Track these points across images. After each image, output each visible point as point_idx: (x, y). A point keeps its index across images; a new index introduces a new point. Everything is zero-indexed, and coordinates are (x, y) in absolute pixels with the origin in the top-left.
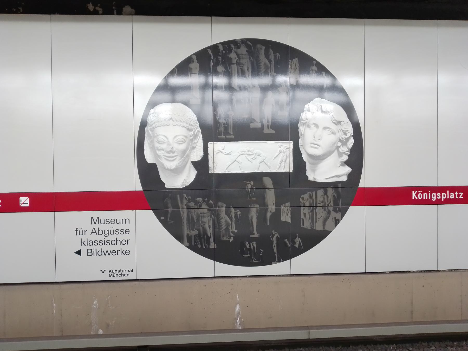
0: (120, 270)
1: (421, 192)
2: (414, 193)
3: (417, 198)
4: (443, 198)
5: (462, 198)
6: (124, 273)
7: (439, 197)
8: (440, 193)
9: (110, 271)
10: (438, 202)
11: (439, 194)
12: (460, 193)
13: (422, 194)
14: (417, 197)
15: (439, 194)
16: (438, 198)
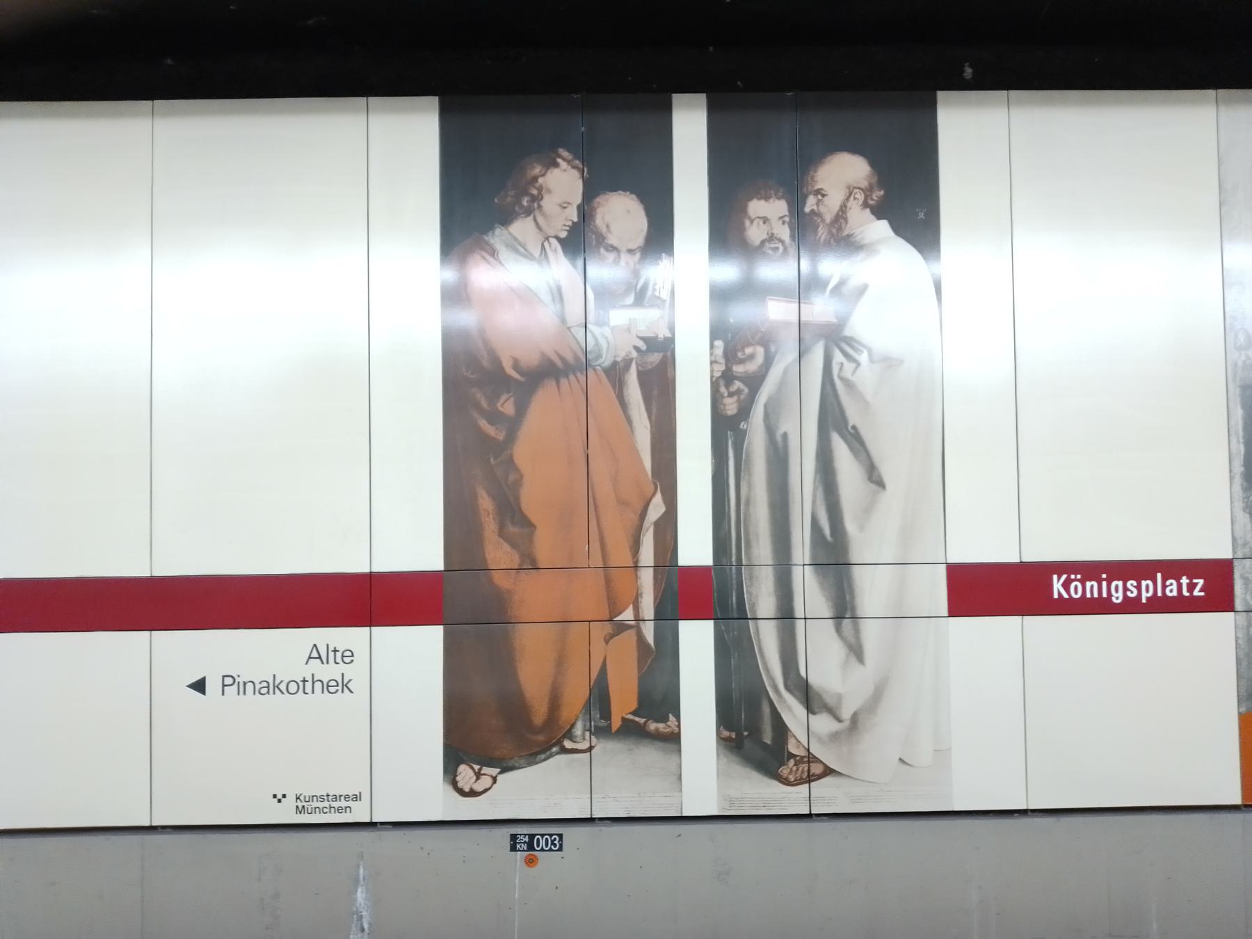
3: (1066, 596)
4: (1145, 595)
5: (1202, 594)
6: (336, 804)
7: (1132, 592)
8: (1136, 581)
10: (1131, 606)
11: (1132, 585)
12: (1195, 581)
13: (1083, 582)
14: (1068, 591)
16: (1129, 594)
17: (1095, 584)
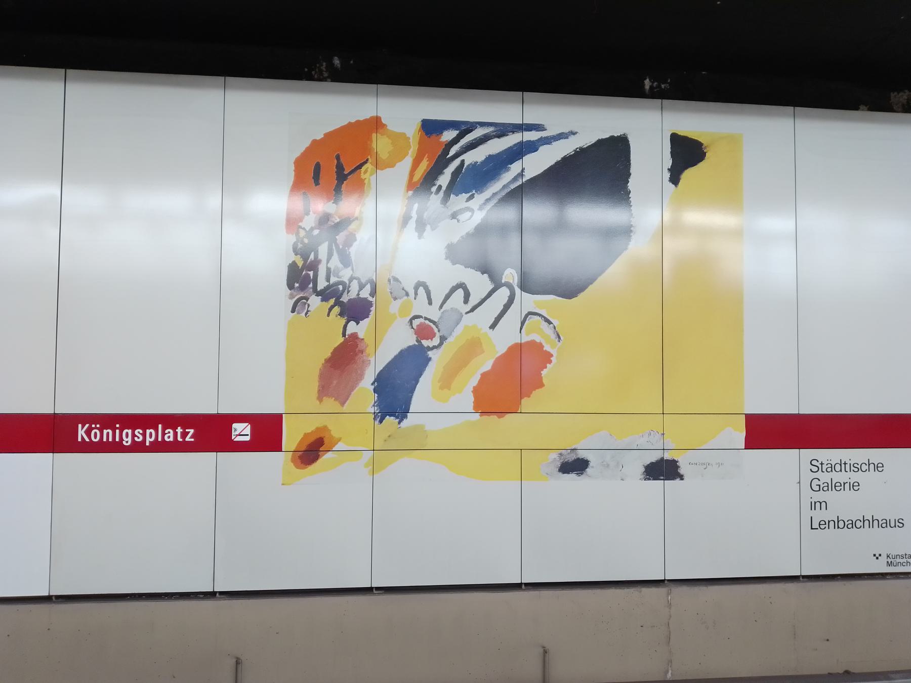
0: (904, 554)
1: (98, 426)
2: (82, 430)
3: (87, 440)
4: (148, 440)
5: (193, 440)
7: (139, 438)
9: (888, 556)
10: (138, 447)
11: (139, 432)
12: (187, 430)
14: (89, 437)
15: (139, 432)
16: (136, 439)
17: (110, 431)
